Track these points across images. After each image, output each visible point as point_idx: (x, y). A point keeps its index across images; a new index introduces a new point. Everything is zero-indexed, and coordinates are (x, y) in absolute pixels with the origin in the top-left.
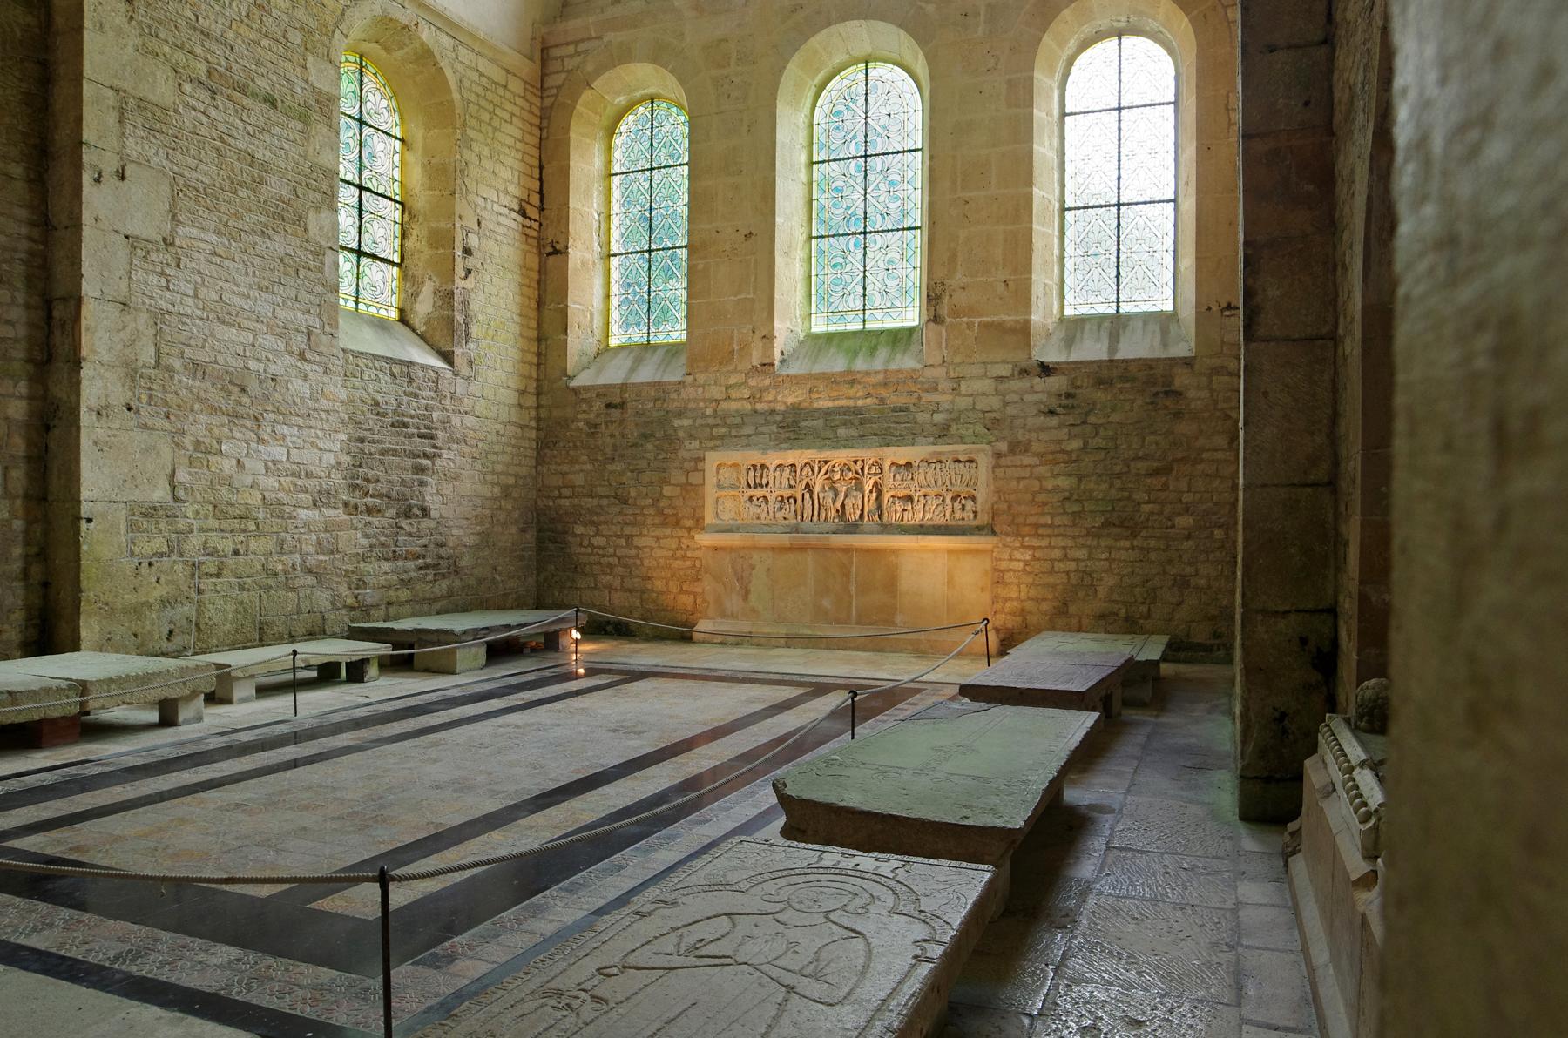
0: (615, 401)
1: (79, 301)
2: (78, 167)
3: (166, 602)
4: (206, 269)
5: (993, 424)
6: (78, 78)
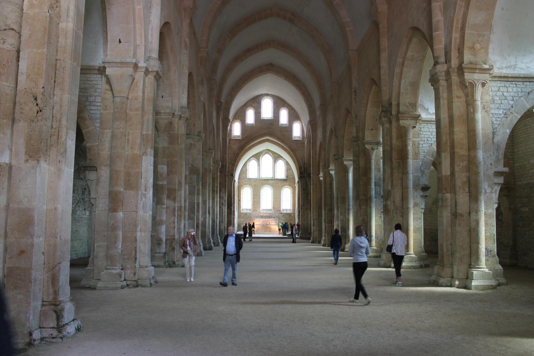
0: (246, 214)
5: (278, 217)
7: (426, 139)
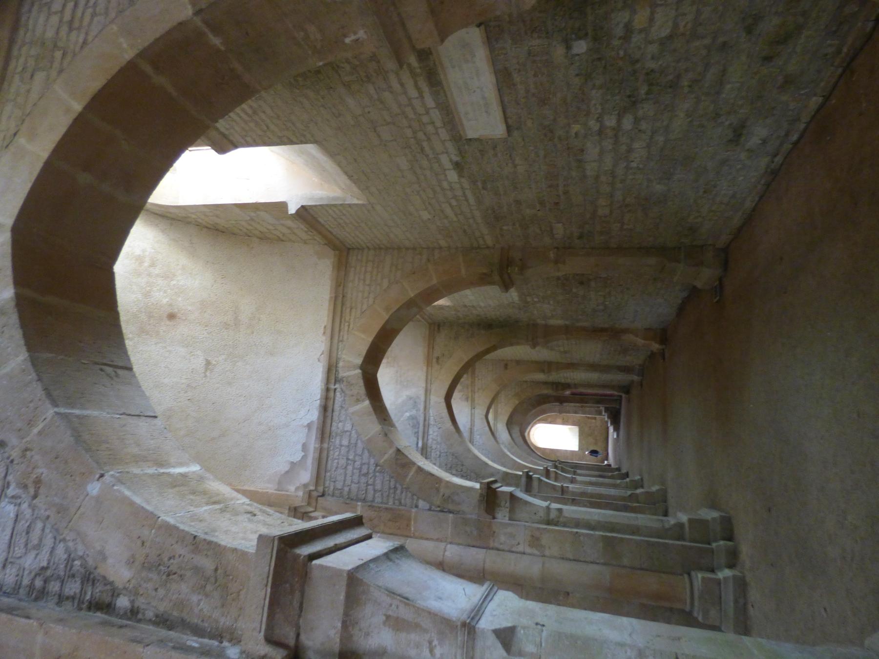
7: (363, 480)
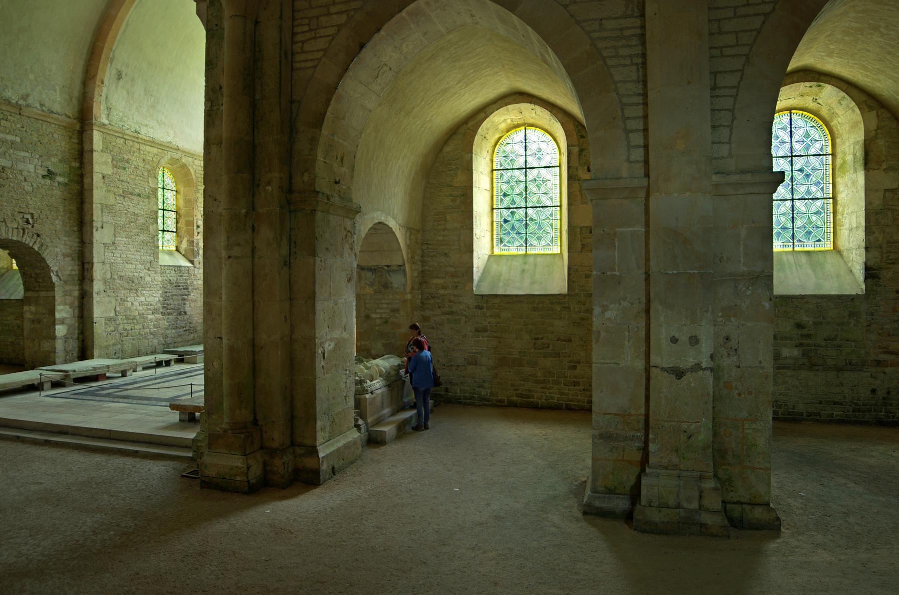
1: (93, 264)
2: (92, 227)
3: (114, 345)
4: (123, 249)
6: (92, 203)
